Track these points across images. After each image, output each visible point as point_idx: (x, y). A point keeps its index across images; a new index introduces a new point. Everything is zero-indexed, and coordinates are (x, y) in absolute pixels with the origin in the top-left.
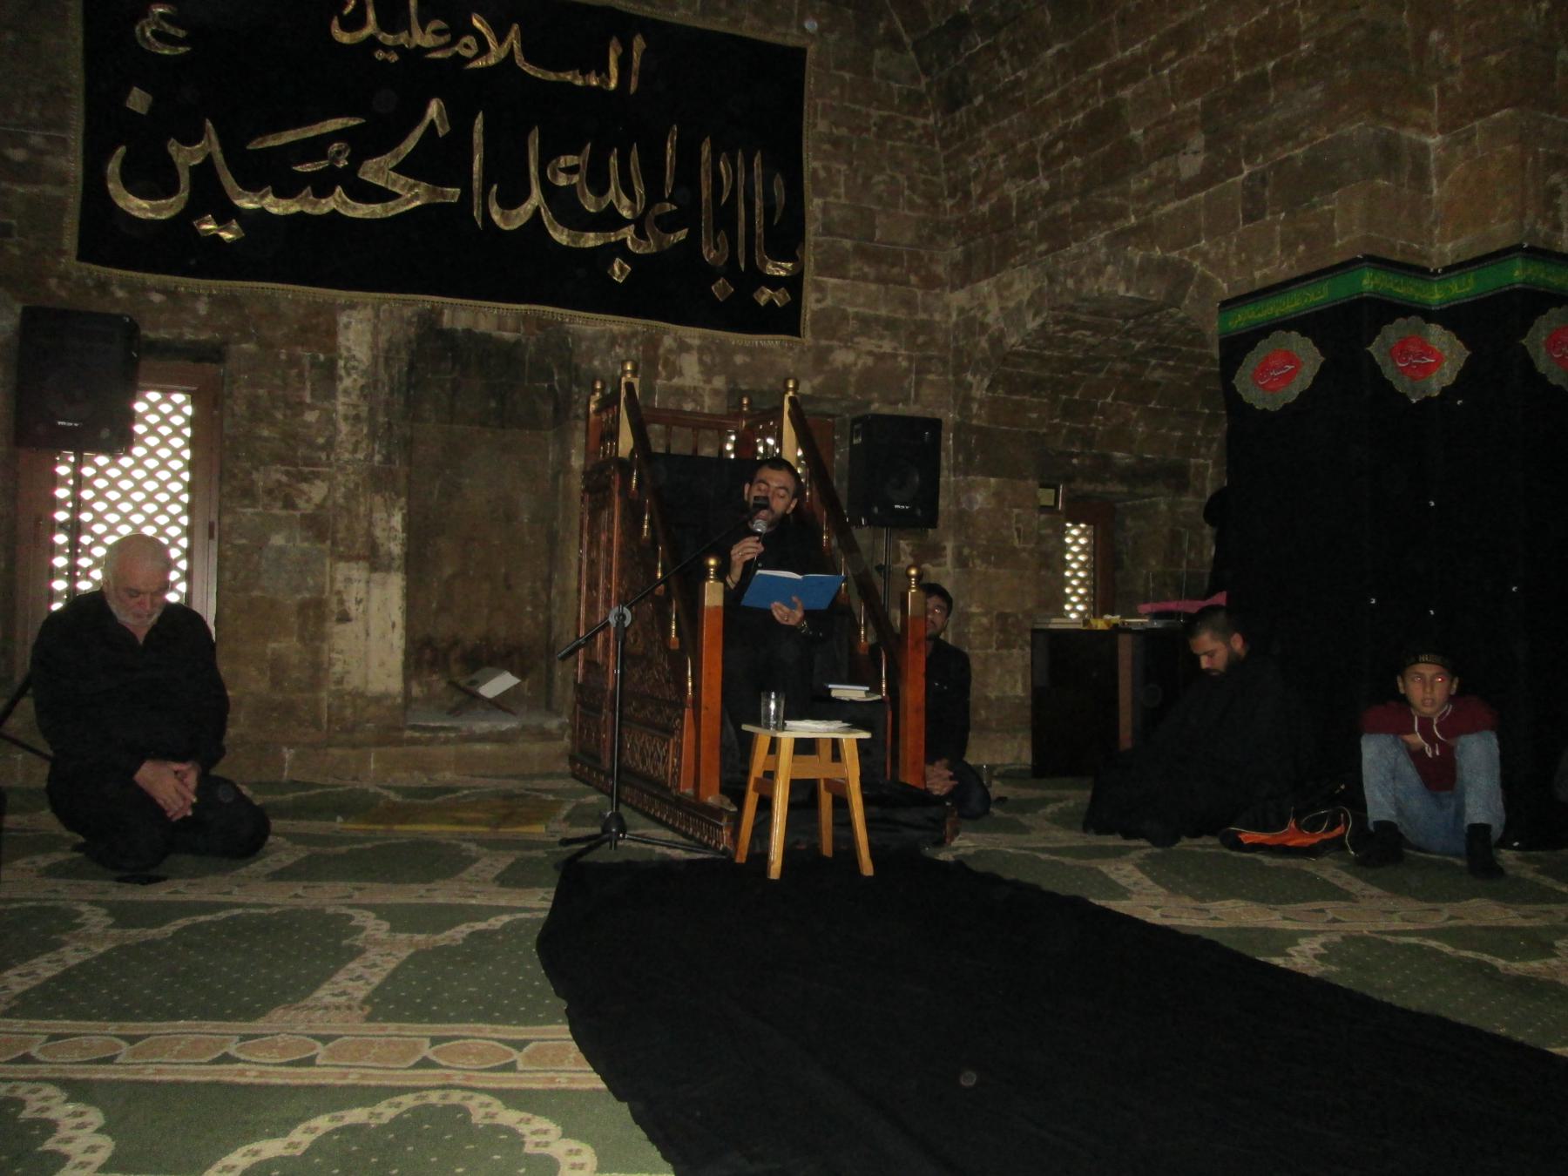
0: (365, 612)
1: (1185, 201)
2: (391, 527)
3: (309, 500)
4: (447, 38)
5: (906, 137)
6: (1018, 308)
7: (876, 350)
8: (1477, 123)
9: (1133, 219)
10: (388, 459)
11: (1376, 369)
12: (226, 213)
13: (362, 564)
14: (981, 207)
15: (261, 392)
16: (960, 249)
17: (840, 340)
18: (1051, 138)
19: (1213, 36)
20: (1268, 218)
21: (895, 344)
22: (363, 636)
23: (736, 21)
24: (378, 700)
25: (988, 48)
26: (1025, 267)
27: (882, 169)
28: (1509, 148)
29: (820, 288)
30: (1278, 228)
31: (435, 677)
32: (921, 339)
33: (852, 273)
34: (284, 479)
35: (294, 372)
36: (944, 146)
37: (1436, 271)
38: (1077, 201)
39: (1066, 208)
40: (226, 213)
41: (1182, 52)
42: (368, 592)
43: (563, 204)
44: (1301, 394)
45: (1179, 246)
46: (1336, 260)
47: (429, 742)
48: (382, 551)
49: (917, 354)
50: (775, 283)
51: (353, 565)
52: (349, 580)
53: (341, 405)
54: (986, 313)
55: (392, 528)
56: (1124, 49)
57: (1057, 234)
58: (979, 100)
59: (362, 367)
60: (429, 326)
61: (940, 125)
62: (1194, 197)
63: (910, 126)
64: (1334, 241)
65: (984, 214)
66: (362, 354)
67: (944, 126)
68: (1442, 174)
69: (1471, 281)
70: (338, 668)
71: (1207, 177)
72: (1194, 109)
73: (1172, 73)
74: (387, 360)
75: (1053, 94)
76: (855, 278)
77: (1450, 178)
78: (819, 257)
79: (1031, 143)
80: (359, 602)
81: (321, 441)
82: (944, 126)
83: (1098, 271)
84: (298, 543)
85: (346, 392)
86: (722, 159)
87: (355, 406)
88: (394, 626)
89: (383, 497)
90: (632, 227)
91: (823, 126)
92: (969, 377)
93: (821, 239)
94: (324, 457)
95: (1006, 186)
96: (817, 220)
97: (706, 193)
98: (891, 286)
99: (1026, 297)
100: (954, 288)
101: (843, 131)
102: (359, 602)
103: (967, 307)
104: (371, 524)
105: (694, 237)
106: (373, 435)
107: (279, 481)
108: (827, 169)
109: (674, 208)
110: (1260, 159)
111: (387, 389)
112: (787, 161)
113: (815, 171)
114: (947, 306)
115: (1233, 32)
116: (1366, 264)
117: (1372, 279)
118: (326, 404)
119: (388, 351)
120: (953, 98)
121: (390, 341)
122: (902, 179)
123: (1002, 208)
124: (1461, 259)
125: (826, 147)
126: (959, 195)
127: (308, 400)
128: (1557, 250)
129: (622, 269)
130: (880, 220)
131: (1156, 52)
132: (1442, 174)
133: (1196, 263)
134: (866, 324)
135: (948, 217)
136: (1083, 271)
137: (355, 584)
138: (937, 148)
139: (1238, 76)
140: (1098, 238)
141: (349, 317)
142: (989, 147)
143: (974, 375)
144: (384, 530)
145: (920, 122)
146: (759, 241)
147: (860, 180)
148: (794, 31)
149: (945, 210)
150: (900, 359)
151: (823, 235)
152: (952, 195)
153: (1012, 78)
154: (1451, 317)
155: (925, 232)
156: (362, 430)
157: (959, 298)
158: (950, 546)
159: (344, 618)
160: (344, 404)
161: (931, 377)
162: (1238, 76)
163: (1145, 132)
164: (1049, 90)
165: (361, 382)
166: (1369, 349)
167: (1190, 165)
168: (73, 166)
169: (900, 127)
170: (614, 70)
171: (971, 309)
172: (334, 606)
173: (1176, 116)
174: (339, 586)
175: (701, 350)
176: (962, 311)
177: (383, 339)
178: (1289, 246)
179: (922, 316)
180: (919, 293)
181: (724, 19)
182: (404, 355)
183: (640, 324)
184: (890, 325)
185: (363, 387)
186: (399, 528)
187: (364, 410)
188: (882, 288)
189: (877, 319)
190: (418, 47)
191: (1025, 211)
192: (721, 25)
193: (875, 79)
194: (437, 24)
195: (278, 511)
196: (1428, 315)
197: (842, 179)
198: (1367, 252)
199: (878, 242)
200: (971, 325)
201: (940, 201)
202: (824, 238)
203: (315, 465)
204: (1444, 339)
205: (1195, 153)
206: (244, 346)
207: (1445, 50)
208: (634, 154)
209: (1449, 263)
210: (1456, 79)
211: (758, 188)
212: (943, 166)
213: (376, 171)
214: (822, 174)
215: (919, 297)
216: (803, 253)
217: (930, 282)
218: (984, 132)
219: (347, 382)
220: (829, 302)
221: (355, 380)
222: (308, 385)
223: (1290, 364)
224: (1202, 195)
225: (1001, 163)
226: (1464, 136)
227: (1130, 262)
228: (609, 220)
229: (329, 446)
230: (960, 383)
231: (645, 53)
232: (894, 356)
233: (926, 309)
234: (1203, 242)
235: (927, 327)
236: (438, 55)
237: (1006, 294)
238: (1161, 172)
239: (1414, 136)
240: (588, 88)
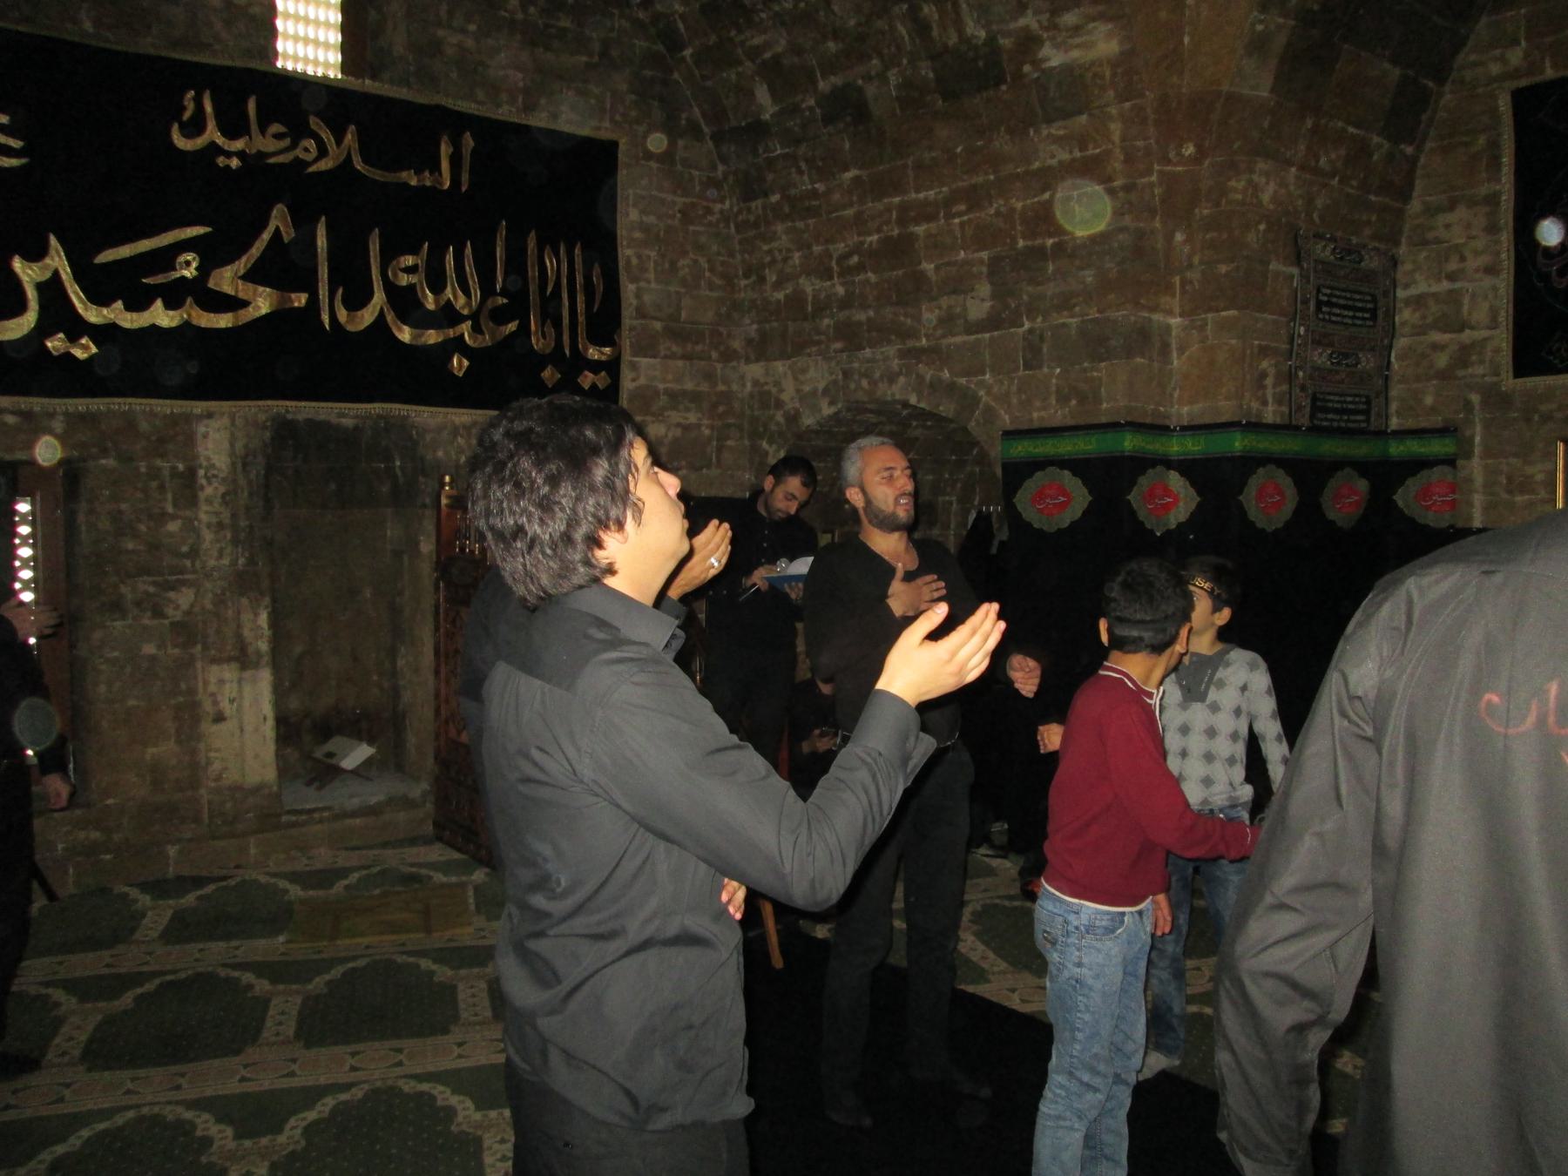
0: (240, 710)
1: (973, 337)
2: (257, 624)
3: (177, 607)
4: (287, 142)
5: (705, 221)
6: (814, 392)
7: (682, 421)
8: (1210, 316)
9: (924, 341)
10: (251, 561)
11: (1133, 513)
12: (76, 327)
13: (234, 665)
14: (775, 294)
15: (124, 506)
16: (755, 326)
17: (653, 415)
18: (847, 249)
19: (998, 204)
20: (1046, 370)
21: (700, 415)
22: (238, 732)
24: (257, 789)
25: (785, 156)
26: (820, 358)
27: (684, 253)
28: (1234, 342)
29: (634, 367)
30: (1054, 381)
31: (289, 750)
32: (721, 409)
33: (662, 353)
34: (151, 589)
35: (154, 484)
36: (738, 231)
37: (1175, 427)
38: (871, 313)
39: (861, 316)
40: (76, 327)
41: (969, 210)
42: (240, 691)
43: (404, 303)
44: (1072, 523)
45: (968, 373)
46: (1104, 420)
47: (303, 824)
48: (251, 650)
49: (718, 423)
50: (596, 367)
51: (225, 666)
53: (204, 515)
54: (782, 391)
55: (259, 627)
56: (918, 191)
57: (851, 336)
58: (775, 198)
59: (221, 475)
60: (285, 430)
61: (735, 209)
62: (980, 336)
63: (709, 211)
64: (1101, 404)
65: (779, 301)
66: (221, 462)
67: (740, 212)
68: (1181, 350)
69: (1202, 441)
71: (993, 322)
72: (981, 262)
73: (962, 225)
74: (245, 465)
75: (849, 212)
76: (666, 357)
77: (1187, 353)
78: (633, 340)
79: (827, 250)
81: (185, 549)
82: (740, 212)
83: (892, 378)
84: (170, 651)
85: (209, 501)
86: (546, 252)
87: (217, 514)
88: (265, 719)
90: (469, 323)
91: (634, 215)
92: (765, 445)
93: (635, 322)
94: (188, 563)
95: (801, 281)
96: (631, 304)
97: (533, 288)
98: (695, 361)
99: (821, 386)
100: (748, 361)
101: (651, 219)
102: (232, 701)
103: (762, 380)
104: (239, 626)
105: (524, 329)
106: (235, 541)
107: (146, 593)
108: (639, 257)
109: (505, 301)
110: (1040, 319)
111: (246, 494)
113: (628, 262)
114: (742, 377)
115: (1019, 205)
116: (1127, 428)
117: (1132, 441)
118: (188, 513)
119: (247, 455)
120: (750, 188)
121: (246, 446)
123: (797, 300)
124: (1192, 423)
125: (637, 235)
126: (754, 278)
127: (170, 510)
128: (1264, 421)
129: (460, 363)
130: (686, 302)
131: (949, 202)
132: (1182, 350)
133: (982, 393)
135: (743, 295)
136: (877, 375)
137: (228, 686)
138: (733, 229)
139: (1021, 243)
140: (891, 350)
141: (207, 426)
142: (784, 241)
143: (770, 443)
144: (252, 630)
145: (718, 207)
146: (581, 329)
147: (667, 266)
148: (607, 124)
149: (740, 290)
150: (703, 428)
151: (636, 318)
152: (746, 276)
153: (809, 187)
154: (1187, 467)
155: (724, 310)
156: (225, 537)
157: (755, 370)
159: (220, 718)
160: (207, 512)
161: (730, 443)
162: (1021, 243)
163: (937, 268)
164: (844, 207)
165: (222, 490)
166: (1129, 497)
167: (978, 306)
169: (700, 212)
170: (445, 165)
171: (766, 383)
172: (208, 706)
173: (966, 262)
174: (212, 688)
176: (756, 383)
177: (239, 445)
178: (1063, 399)
179: (721, 387)
180: (719, 366)
181: (544, 115)
182: (260, 459)
185: (224, 496)
186: (265, 626)
187: (226, 516)
188: (688, 363)
189: (684, 393)
190: (259, 152)
191: (821, 308)
193: (679, 167)
194: (276, 128)
195: (146, 621)
196: (1168, 463)
197: (652, 264)
198: (1129, 419)
199: (684, 322)
200: (765, 398)
201: (736, 281)
202: (639, 322)
203: (181, 573)
204: (1181, 483)
205: (983, 300)
206: (103, 462)
207: (1187, 249)
208: (468, 250)
209: (1186, 424)
210: (1194, 275)
211: (579, 279)
212: (737, 247)
213: (226, 280)
214: (634, 261)
215: (719, 370)
216: (620, 337)
217: (728, 356)
218: (779, 228)
219: (209, 491)
220: (642, 381)
221: (216, 488)
222: (169, 496)
223: (1063, 496)
224: (987, 335)
225: (797, 257)
226: (1199, 323)
227: (920, 377)
228: (448, 316)
229: (194, 553)
230: (755, 449)
231: (474, 152)
232: (698, 426)
233: (726, 382)
234: (988, 376)
235: (727, 397)
236: (281, 159)
237: (801, 377)
238: (950, 307)
239: (1161, 319)
240: (422, 189)
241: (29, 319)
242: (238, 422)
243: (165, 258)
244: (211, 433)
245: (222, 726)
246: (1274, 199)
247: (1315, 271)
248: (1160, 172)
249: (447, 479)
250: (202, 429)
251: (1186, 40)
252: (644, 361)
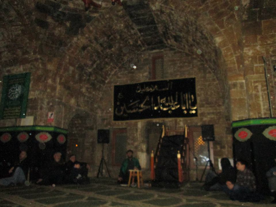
23: (185, 77)
29: (201, 110)
112: (194, 93)
113: (198, 94)
122: (213, 91)
125: (200, 90)
134: (209, 114)
158: (226, 146)
168: (112, 111)
175: (183, 121)
179: (218, 111)
184: (213, 113)
192: (183, 77)
213: (142, 106)
217: (219, 106)
220: (202, 111)
232: (214, 118)
241: (122, 113)
243: (135, 104)
246: (253, 53)
247: (272, 63)
248: (236, 57)
251: (235, 33)
252: (202, 108)
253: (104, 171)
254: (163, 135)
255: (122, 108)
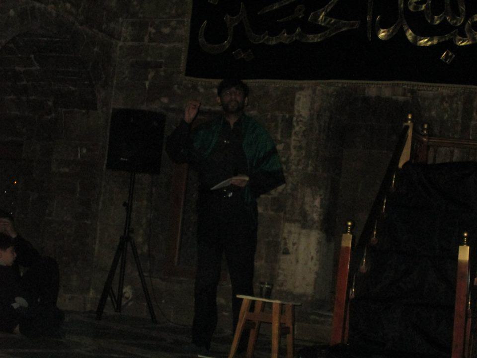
35: (273, 125)
51: (293, 224)
52: (290, 232)
53: (294, 141)
70: (281, 278)
80: (294, 244)
88: (312, 258)
89: (311, 189)
90: (457, 30)
102: (294, 244)
111: (317, 132)
118: (288, 140)
127: (279, 139)
141: (300, 94)
144: (310, 206)
156: (302, 154)
159: (286, 252)
160: (294, 140)
165: (304, 128)
168: (184, 32)
172: (282, 246)
174: (285, 235)
183: (459, 88)
185: (304, 131)
219: (297, 129)
242: (317, 92)
244: (302, 98)
245: (288, 257)
249: (426, 126)
250: (297, 96)
253: (128, 291)
254: (405, 157)
255: (227, 18)
